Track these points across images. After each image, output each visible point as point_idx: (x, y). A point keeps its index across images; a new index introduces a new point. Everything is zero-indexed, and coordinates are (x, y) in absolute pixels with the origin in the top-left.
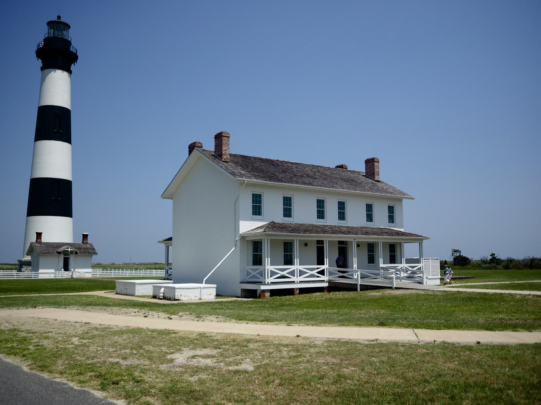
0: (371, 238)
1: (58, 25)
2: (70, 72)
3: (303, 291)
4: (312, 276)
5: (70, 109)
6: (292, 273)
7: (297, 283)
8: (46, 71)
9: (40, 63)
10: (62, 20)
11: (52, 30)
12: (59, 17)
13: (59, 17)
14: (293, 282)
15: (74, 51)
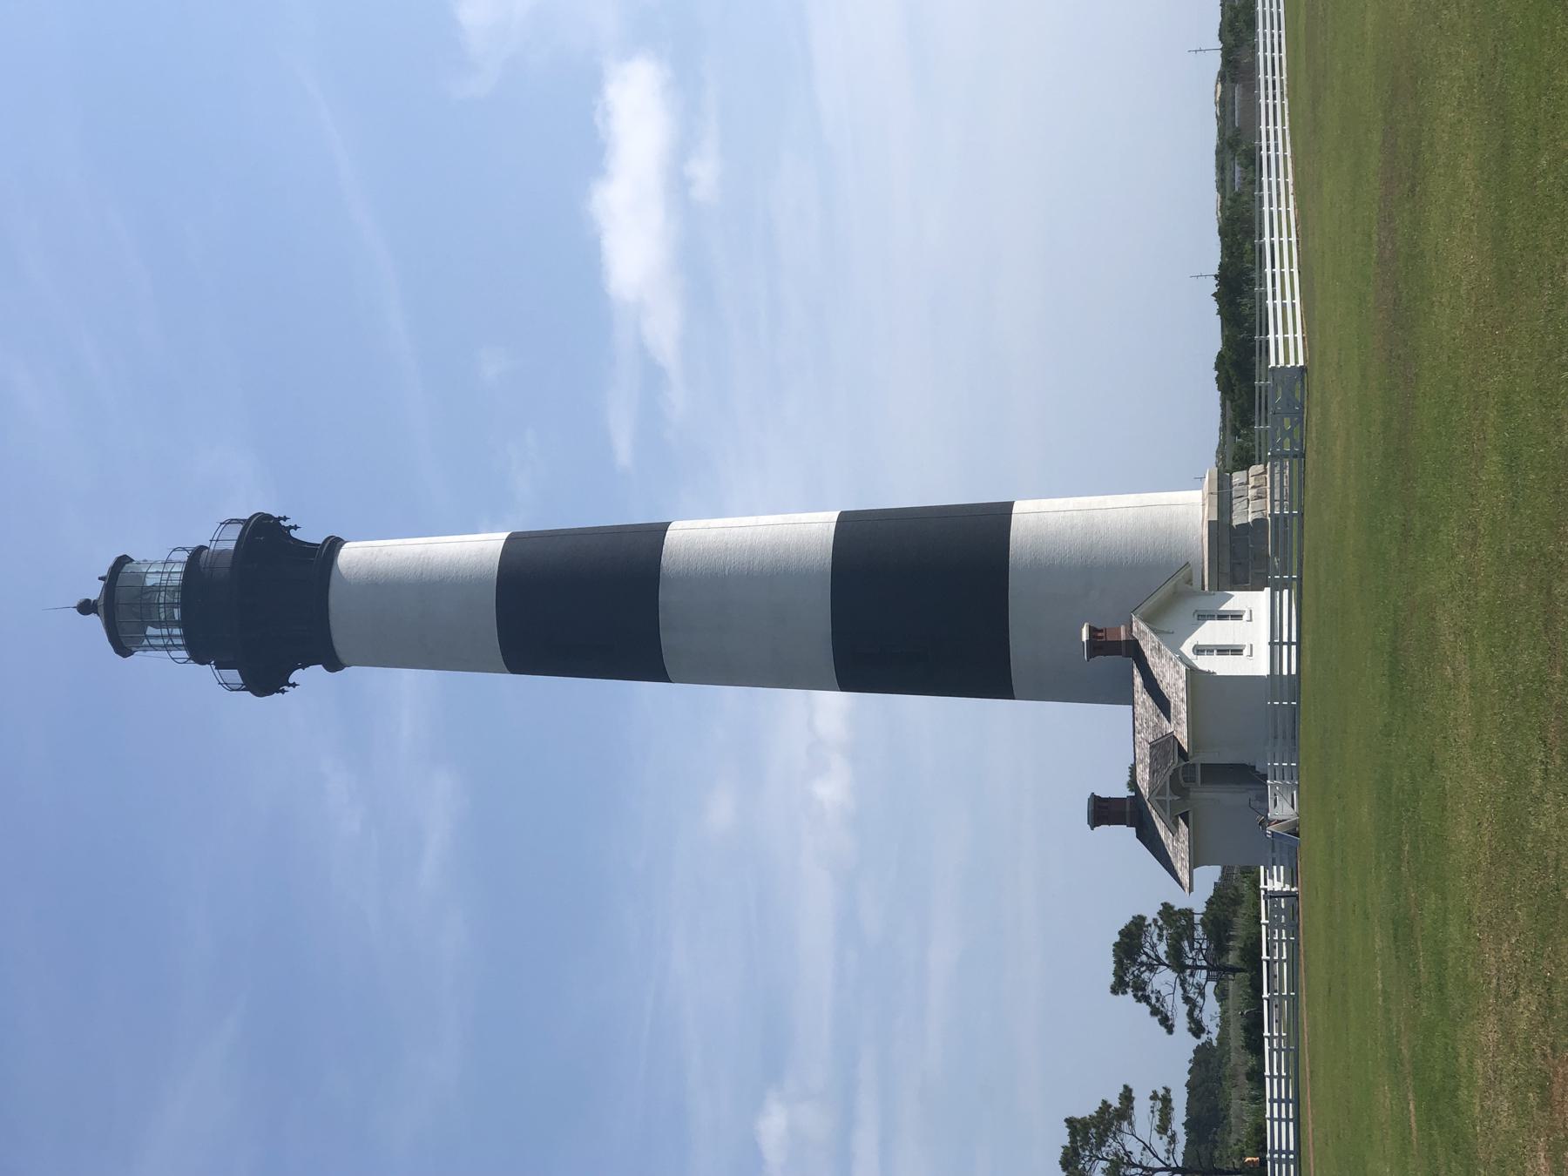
1: (122, 609)
5: (505, 535)
8: (339, 646)
9: (309, 678)
10: (95, 591)
11: (151, 631)
12: (86, 607)
13: (86, 607)
15: (235, 532)
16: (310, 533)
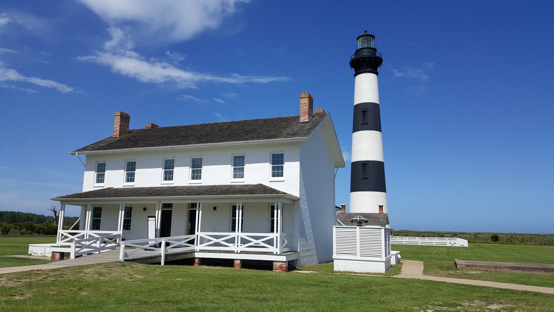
0: (167, 199)
2: (377, 73)
3: (246, 264)
4: (216, 244)
6: (232, 241)
7: (237, 253)
9: (353, 71)
10: (368, 33)
14: (232, 252)
16: (379, 69)
